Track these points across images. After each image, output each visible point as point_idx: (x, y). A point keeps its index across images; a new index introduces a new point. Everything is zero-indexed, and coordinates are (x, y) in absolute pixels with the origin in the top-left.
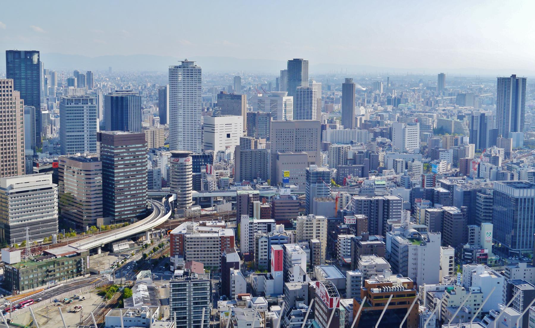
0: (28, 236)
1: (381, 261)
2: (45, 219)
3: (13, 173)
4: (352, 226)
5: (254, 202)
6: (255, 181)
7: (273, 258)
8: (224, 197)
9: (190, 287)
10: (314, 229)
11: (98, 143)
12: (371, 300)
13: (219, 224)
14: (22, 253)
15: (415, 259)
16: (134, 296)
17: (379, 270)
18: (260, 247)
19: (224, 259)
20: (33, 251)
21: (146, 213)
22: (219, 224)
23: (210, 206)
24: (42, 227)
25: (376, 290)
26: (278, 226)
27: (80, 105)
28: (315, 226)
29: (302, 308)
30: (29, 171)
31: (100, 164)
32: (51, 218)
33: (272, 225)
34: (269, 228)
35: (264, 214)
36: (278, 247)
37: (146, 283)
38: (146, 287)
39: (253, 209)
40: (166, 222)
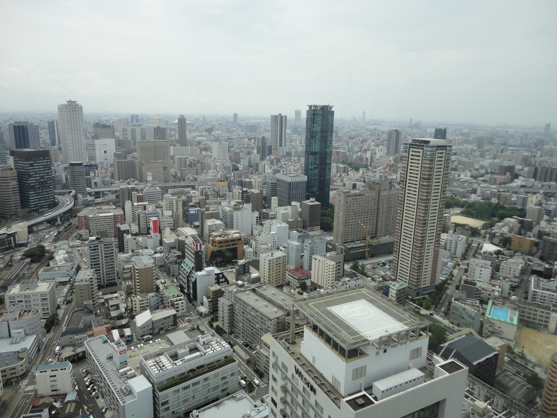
1: (218, 222)
4: (197, 203)
8: (109, 191)
9: (101, 247)
10: (175, 206)
11: (11, 158)
12: (217, 244)
13: (111, 207)
15: (237, 220)
16: (57, 258)
17: (217, 227)
18: (141, 220)
21: (54, 205)
22: (111, 207)
23: (99, 197)
25: (218, 239)
26: (151, 206)
28: (175, 204)
29: (175, 253)
31: (15, 171)
35: (140, 199)
36: (155, 219)
37: (64, 249)
38: (64, 252)
40: (71, 209)
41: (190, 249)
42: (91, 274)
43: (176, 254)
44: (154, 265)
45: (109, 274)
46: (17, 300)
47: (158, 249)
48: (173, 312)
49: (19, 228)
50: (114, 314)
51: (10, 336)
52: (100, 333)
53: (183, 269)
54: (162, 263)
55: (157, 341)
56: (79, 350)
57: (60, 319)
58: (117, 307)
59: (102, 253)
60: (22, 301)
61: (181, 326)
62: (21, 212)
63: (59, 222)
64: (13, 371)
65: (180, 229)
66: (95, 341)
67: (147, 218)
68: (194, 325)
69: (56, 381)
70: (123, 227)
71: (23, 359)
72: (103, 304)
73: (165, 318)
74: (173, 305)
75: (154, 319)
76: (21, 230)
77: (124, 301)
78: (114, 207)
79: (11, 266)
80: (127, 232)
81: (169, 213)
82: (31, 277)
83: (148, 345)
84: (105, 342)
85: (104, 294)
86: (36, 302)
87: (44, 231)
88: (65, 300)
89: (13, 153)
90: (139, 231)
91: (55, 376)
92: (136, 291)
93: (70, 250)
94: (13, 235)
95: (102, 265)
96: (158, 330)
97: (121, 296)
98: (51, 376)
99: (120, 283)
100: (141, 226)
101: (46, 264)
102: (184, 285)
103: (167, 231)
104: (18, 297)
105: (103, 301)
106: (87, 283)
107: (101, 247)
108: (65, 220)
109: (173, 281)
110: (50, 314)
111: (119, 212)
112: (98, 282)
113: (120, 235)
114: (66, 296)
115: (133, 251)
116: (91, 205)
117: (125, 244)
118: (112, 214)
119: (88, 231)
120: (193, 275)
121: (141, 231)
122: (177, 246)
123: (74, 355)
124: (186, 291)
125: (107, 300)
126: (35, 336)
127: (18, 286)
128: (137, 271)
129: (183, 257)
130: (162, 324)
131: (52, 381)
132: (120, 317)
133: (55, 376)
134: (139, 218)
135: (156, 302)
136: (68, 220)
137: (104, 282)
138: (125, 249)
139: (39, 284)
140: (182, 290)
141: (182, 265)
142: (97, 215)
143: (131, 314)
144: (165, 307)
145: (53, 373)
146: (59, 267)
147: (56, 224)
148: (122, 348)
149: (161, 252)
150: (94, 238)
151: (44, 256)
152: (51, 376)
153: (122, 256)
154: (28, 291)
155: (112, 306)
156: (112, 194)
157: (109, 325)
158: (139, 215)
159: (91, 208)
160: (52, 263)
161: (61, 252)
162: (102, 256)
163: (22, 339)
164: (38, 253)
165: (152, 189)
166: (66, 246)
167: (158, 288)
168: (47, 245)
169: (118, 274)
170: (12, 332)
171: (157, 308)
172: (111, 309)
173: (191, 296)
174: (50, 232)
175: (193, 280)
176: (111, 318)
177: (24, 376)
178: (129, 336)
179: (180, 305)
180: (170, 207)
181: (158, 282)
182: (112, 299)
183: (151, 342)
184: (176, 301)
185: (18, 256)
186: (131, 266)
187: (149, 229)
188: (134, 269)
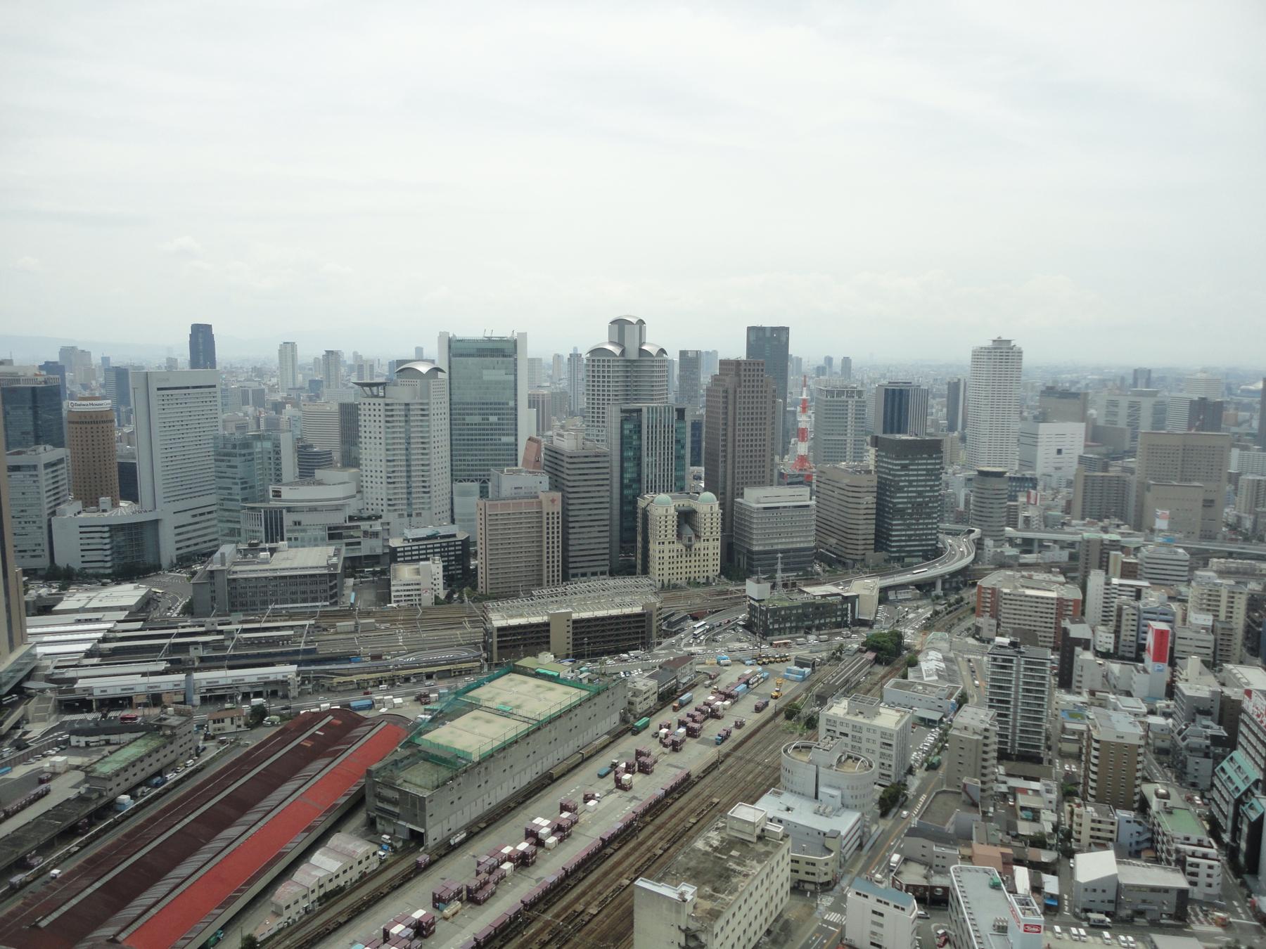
0: (779, 566)
2: (798, 546)
3: (761, 483)
5: (1113, 553)
6: (1106, 521)
7: (1150, 640)
8: (1055, 542)
9: (1019, 665)
11: (872, 451)
14: (773, 587)
19: (1066, 631)
20: (785, 586)
21: (934, 554)
23: (1030, 552)
24: (794, 557)
26: (1156, 594)
27: (844, 398)
29: (1207, 727)
30: (779, 484)
32: (806, 545)
33: (1144, 590)
34: (1138, 594)
35: (1129, 571)
37: (939, 650)
38: (940, 656)
39: (1108, 562)
40: (966, 568)
41: (1255, 729)
42: (988, 719)
43: (1209, 732)
44: (1142, 742)
45: (1027, 732)
46: (839, 729)
47: (1161, 704)
48: (1178, 881)
49: (865, 587)
50: (1025, 828)
51: (816, 797)
52: (987, 861)
53: (1224, 777)
54: (1166, 744)
55: (1122, 938)
56: (937, 881)
57: (910, 797)
58: (1035, 816)
59: (1018, 678)
60: (846, 735)
61: (1197, 927)
62: (873, 557)
63: (939, 591)
64: (811, 869)
65: (1230, 666)
66: (974, 874)
67: (1141, 618)
68: (1237, 941)
69: (881, 925)
70: (1077, 631)
71: (830, 851)
72: (1004, 796)
73: (1154, 890)
74: (1181, 863)
75: (1124, 880)
76: (867, 592)
77: (1054, 806)
78: (1062, 579)
79: (839, 659)
80: (1086, 644)
81: (1206, 619)
82: (869, 691)
83: (1098, 939)
84: (996, 886)
85: (1008, 775)
86: (870, 746)
87: (909, 604)
88: (926, 760)
89: (876, 442)
90: (1116, 648)
91: (881, 915)
92: (1085, 791)
93: (952, 655)
94: (852, 600)
95: (1016, 706)
96: (1129, 912)
97: (1048, 791)
98: (874, 912)
99: (1050, 762)
100: (1122, 637)
101: (901, 672)
102: (1222, 820)
103: (1192, 665)
104: (842, 724)
105: (1004, 788)
106: (976, 737)
107: (1019, 665)
108: (950, 589)
109: (1190, 800)
110: (893, 779)
111: (1072, 593)
112: (1000, 742)
113: (1067, 646)
114: (929, 753)
115: (1092, 693)
116: (1010, 567)
117: (1076, 671)
118: (1053, 595)
119: (994, 622)
120: (1254, 801)
121: (1121, 648)
122: (1216, 710)
123: (925, 888)
124: (1226, 838)
125: (1014, 791)
126: (857, 815)
127: (845, 702)
128: (1095, 745)
129: (1230, 743)
130: (1144, 901)
131: (874, 923)
132: (1038, 842)
133: (881, 915)
134: (1119, 616)
135: (1136, 838)
136: (957, 589)
137: (1013, 747)
138: (1075, 684)
139: (881, 710)
140: (1215, 831)
141: (1225, 764)
142: (1021, 590)
143: (1067, 844)
144: (1157, 860)
145: (881, 908)
146: (924, 685)
147: (933, 594)
148: (1032, 919)
149: (1167, 715)
150: (1005, 641)
151: (900, 654)
152: (874, 912)
153: (1065, 698)
154: (860, 719)
155: (1023, 808)
156: (1062, 548)
157: (1009, 851)
158: (1120, 609)
159: (1009, 573)
160: (911, 674)
161: (933, 654)
162: (1017, 686)
163: (836, 812)
164: (890, 645)
165: (1164, 550)
166: (945, 645)
167: (1144, 806)
168: (910, 636)
169: (1048, 738)
170: (822, 789)
171: (1136, 854)
172: (1022, 814)
173: (1242, 859)
174: (918, 608)
175: (1254, 816)
176: (1017, 837)
177: (827, 887)
178: (1052, 896)
179: (1203, 871)
180: (1210, 604)
181: (1148, 789)
182: (1024, 791)
183: (1106, 934)
184: (1193, 855)
185: (855, 641)
186: (1083, 727)
187: (1142, 648)
188: (1090, 738)
